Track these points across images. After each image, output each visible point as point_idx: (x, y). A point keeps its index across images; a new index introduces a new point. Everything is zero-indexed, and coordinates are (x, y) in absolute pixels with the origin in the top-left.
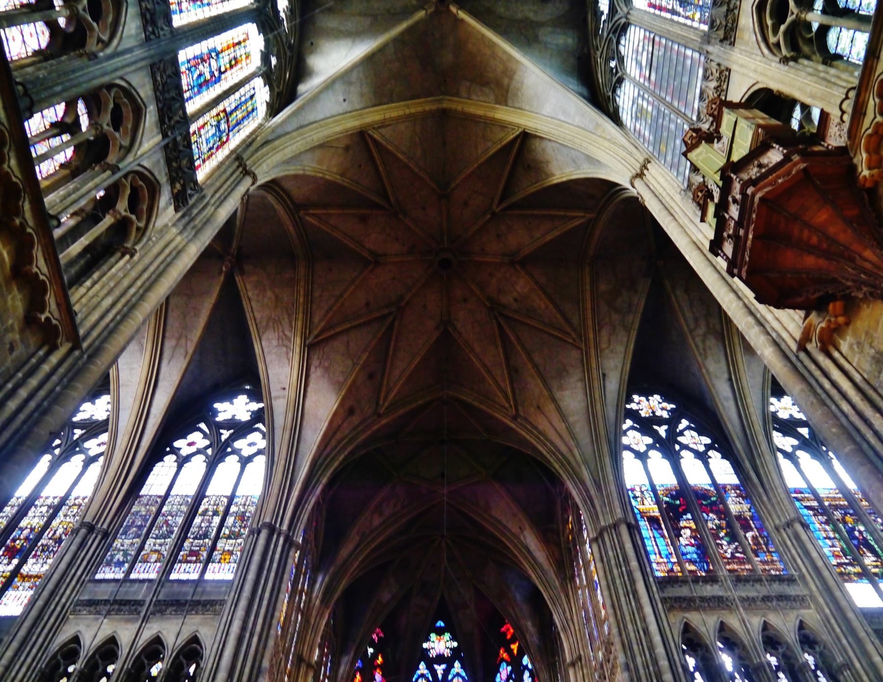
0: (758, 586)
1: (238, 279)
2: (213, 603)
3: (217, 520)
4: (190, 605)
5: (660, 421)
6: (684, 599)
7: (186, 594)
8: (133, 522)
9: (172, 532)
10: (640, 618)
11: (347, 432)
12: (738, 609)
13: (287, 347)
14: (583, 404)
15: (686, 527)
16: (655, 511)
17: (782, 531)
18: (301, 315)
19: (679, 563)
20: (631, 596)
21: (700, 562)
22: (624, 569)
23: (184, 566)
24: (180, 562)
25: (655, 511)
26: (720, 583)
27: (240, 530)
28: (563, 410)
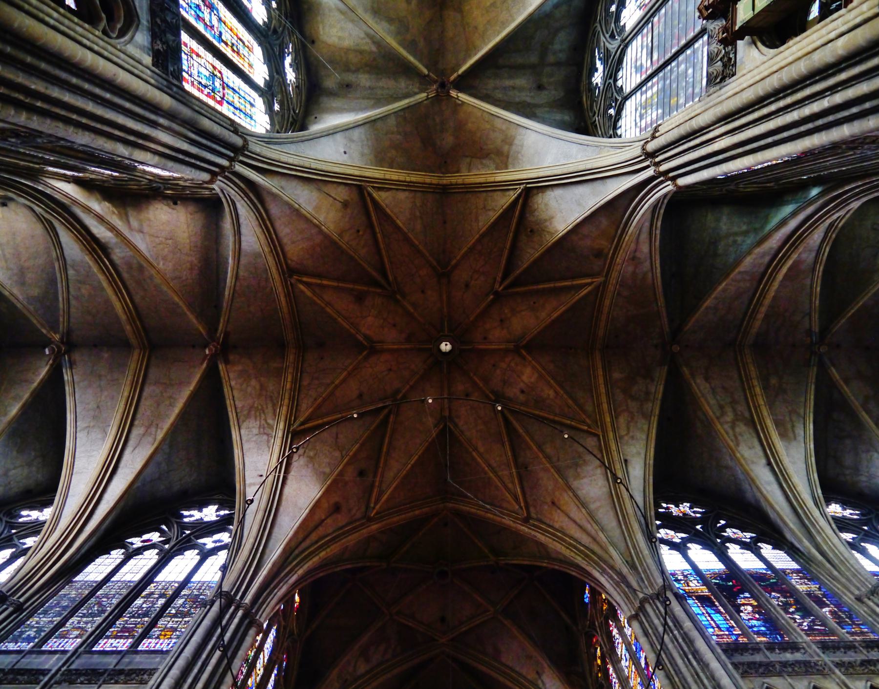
0: (851, 653)
1: (221, 367)
2: (143, 671)
3: (162, 601)
4: (108, 675)
5: (695, 521)
6: (761, 664)
7: (110, 664)
8: (58, 603)
9: (104, 611)
10: (707, 678)
11: (330, 530)
12: (834, 673)
13: (268, 435)
14: (606, 490)
15: (744, 605)
16: (705, 591)
17: (866, 600)
18: (286, 401)
19: (744, 634)
20: (690, 657)
21: (771, 634)
22: (676, 632)
23: (111, 641)
24: (108, 637)
25: (705, 591)
26: (803, 651)
27: (190, 610)
28: (582, 498)
